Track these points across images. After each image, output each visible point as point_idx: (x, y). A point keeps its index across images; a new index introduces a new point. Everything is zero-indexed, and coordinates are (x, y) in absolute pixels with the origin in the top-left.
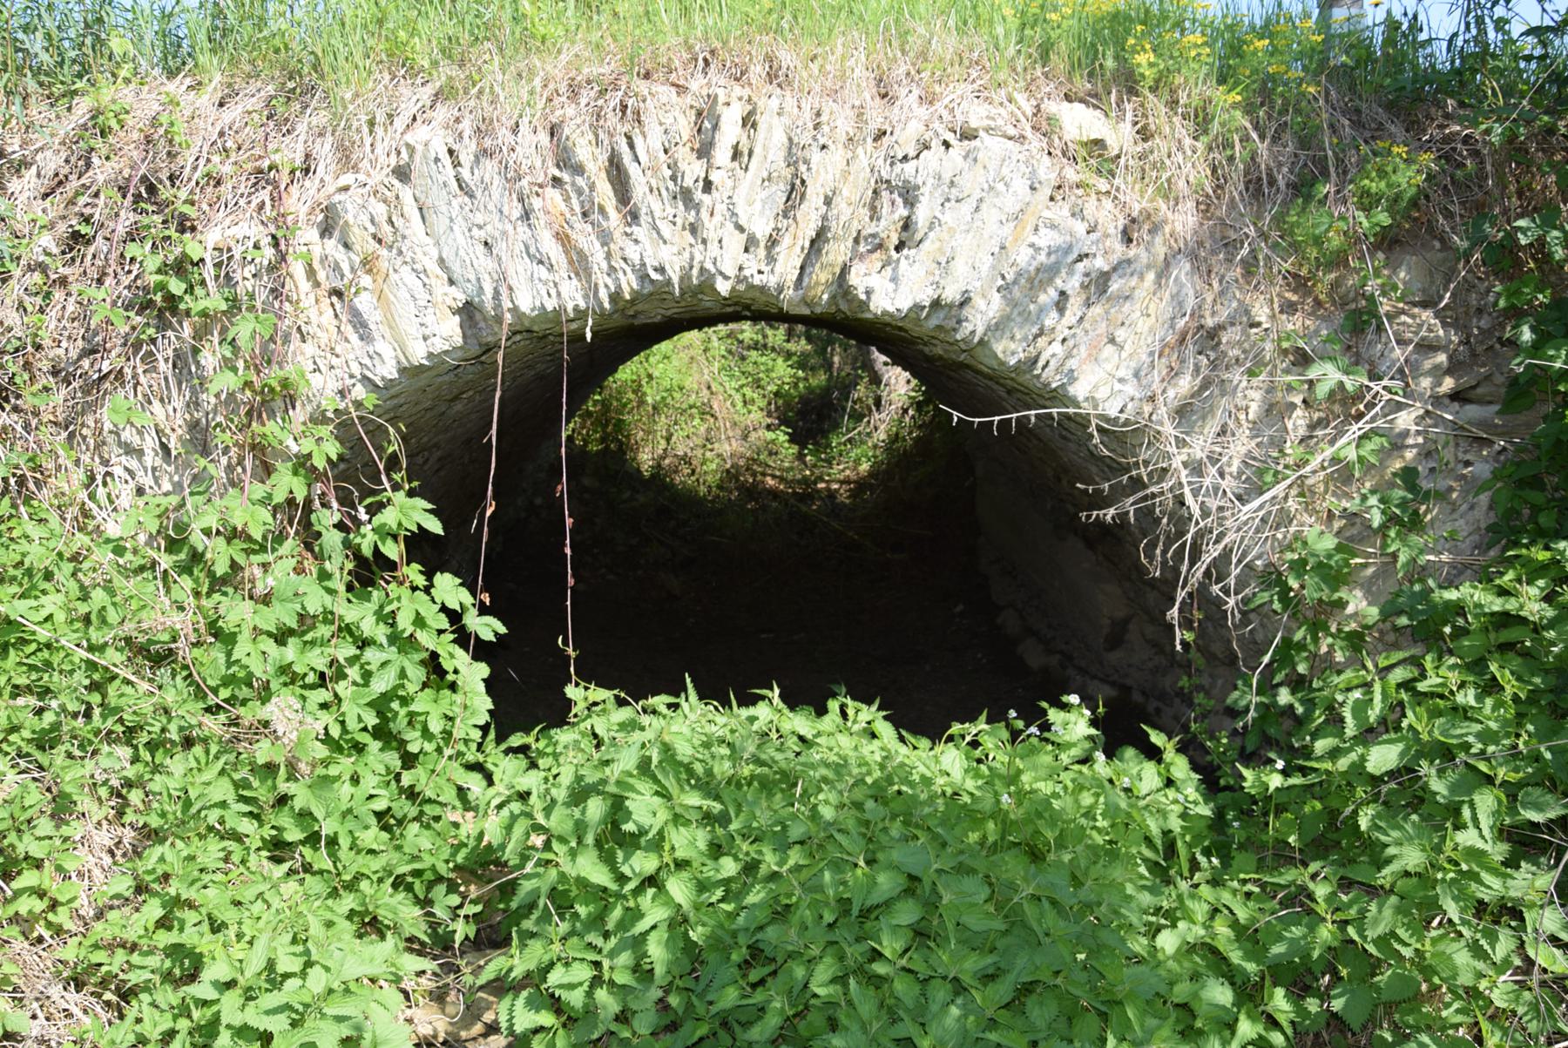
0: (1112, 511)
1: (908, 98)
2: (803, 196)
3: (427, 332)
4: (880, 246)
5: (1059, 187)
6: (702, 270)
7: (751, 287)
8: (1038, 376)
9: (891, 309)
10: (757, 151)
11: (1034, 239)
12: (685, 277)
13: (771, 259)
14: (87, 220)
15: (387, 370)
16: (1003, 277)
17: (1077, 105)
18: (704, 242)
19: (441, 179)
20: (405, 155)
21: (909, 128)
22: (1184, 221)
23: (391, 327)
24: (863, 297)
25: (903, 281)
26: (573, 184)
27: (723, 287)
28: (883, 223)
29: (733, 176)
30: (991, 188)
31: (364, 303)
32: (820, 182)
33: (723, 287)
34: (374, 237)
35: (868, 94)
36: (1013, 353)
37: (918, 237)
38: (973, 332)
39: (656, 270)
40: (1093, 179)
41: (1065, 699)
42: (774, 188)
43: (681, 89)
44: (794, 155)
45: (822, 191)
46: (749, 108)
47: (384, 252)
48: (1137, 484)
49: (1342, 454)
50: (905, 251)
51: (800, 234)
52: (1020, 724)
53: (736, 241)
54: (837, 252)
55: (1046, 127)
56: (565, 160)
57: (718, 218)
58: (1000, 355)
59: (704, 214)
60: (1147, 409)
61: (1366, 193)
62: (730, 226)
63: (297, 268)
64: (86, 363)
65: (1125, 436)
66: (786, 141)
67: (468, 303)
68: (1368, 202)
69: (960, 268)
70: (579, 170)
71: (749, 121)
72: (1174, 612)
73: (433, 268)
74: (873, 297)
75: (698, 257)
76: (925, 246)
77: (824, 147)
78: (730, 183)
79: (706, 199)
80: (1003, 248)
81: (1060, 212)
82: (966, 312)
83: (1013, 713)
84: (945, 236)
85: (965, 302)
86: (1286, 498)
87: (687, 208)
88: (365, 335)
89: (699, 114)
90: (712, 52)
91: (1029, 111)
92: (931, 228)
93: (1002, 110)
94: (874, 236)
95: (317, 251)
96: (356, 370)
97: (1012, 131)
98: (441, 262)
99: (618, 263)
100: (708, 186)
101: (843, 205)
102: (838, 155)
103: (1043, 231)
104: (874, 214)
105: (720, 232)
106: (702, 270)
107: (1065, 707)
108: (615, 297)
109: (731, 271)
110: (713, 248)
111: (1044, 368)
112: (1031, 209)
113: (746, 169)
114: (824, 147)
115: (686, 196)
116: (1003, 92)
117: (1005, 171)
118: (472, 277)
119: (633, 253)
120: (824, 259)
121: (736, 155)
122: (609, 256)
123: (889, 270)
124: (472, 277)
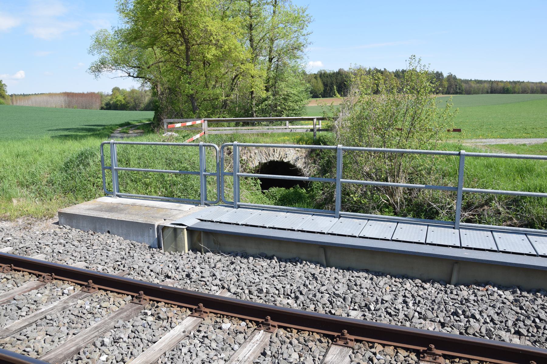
22: (304, 155)
54: (282, 158)
65: (300, 169)
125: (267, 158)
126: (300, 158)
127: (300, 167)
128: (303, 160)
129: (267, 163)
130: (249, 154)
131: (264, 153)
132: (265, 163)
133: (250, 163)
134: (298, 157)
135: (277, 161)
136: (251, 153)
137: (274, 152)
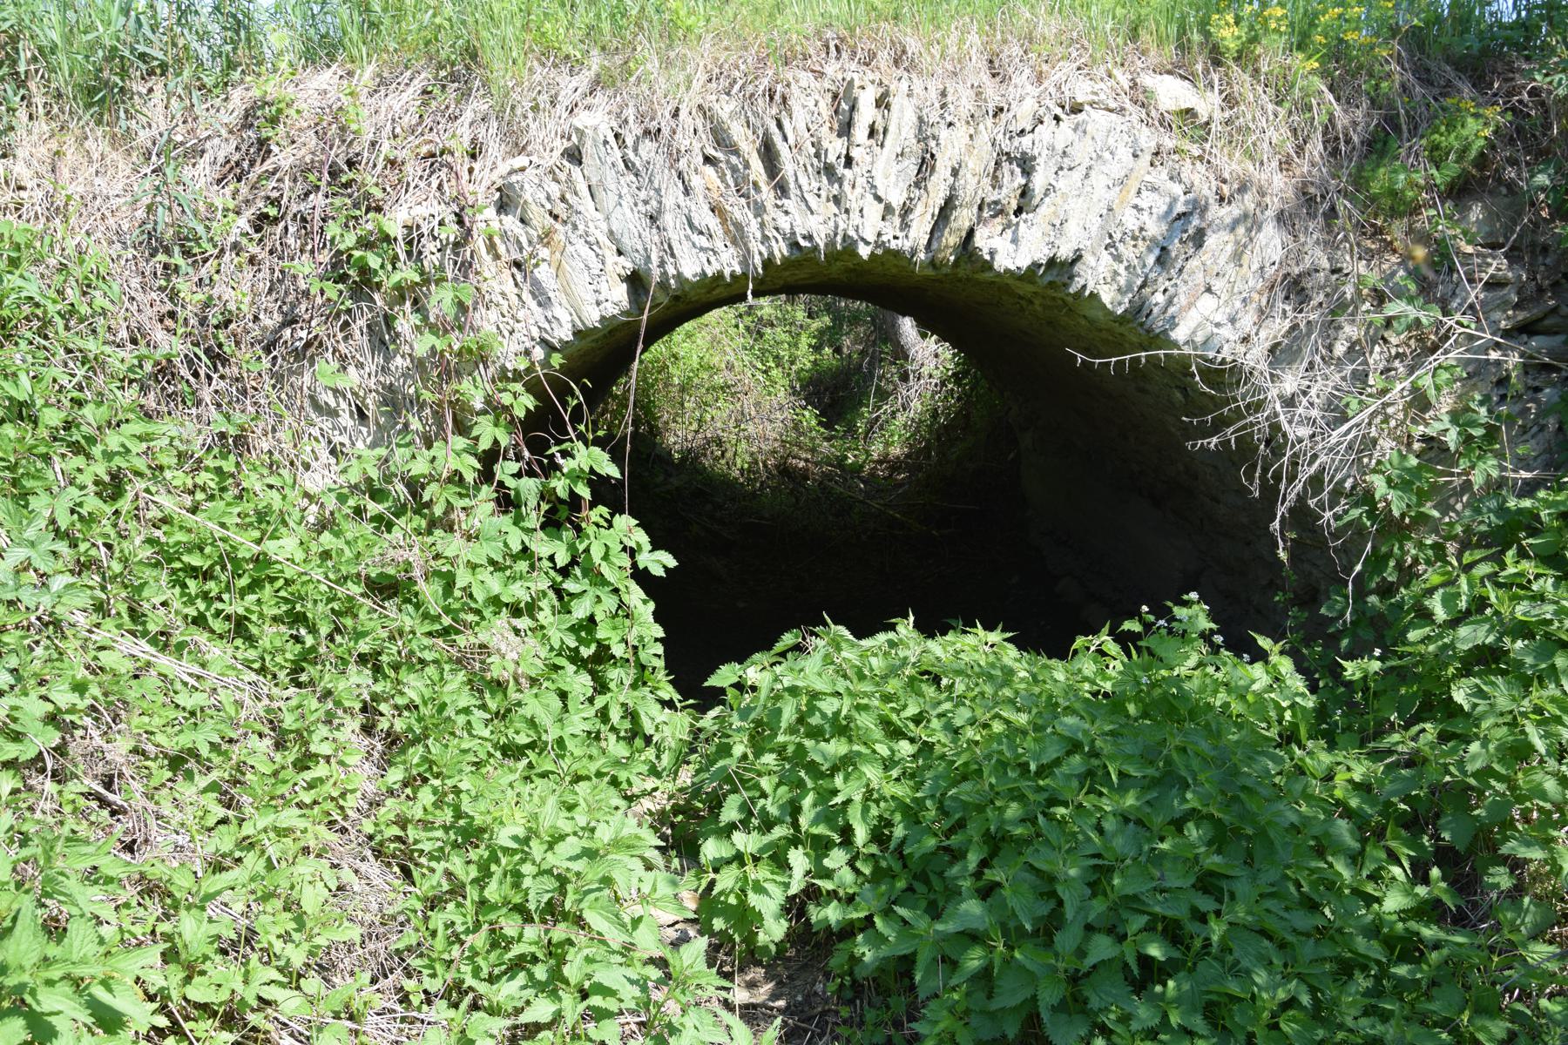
0: (1215, 440)
1: (1022, 79)
2: (933, 168)
3: (601, 298)
4: (1001, 212)
5: (1157, 154)
6: (846, 237)
7: (888, 251)
8: (1142, 324)
9: (1013, 268)
10: (892, 129)
11: (1137, 201)
12: (831, 243)
13: (905, 226)
14: (275, 202)
15: (564, 333)
16: (1111, 236)
17: (1166, 76)
18: (847, 211)
19: (609, 160)
20: (574, 139)
21: (1025, 102)
23: (567, 294)
24: (987, 257)
25: (1023, 243)
26: (728, 162)
27: (864, 251)
28: (1004, 190)
29: (870, 151)
30: (1099, 157)
31: (544, 273)
32: (948, 154)
33: (864, 251)
34: (551, 213)
35: (985, 77)
36: (1120, 304)
37: (1035, 201)
38: (1084, 287)
39: (804, 237)
40: (1186, 145)
41: (1185, 597)
42: (906, 162)
43: (820, 75)
44: (923, 129)
45: (949, 164)
46: (881, 90)
47: (558, 226)
49: (1420, 383)
50: (1024, 216)
51: (931, 202)
52: (1151, 618)
54: (963, 218)
55: (1142, 98)
56: (721, 138)
57: (859, 190)
58: (1109, 306)
59: (847, 187)
60: (1241, 349)
61: (1435, 147)
62: (870, 197)
63: (479, 244)
64: (287, 332)
65: (1224, 376)
66: (915, 119)
67: (634, 272)
68: (1437, 156)
69: (1072, 228)
71: (882, 103)
72: (1276, 524)
73: (604, 239)
74: (997, 257)
75: (842, 226)
76: (1042, 210)
77: (950, 124)
78: (868, 159)
79: (847, 172)
80: (1110, 210)
81: (1160, 176)
82: (1077, 268)
83: (1145, 608)
84: (1059, 201)
85: (1078, 258)
86: (1370, 424)
87: (831, 182)
88: (544, 302)
89: (835, 96)
90: (842, 40)
91: (1126, 85)
92: (1046, 195)
93: (1102, 85)
94: (996, 203)
95: (495, 225)
96: (536, 333)
97: (1113, 105)
98: (611, 232)
99: (771, 233)
100: (849, 162)
101: (969, 176)
102: (962, 131)
103: (1145, 193)
104: (996, 183)
105: (861, 203)
106: (846, 237)
107: (1187, 604)
108: (768, 263)
109: (871, 238)
110: (855, 218)
111: (1148, 316)
112: (1133, 176)
113: (882, 146)
114: (950, 124)
115: (829, 170)
116: (1102, 69)
117: (1111, 141)
118: (640, 248)
119: (783, 221)
120: (953, 225)
121: (872, 133)
122: (762, 225)
123: (1009, 232)
124: (640, 248)
125: (739, 210)
126: (1218, 213)
128: (1271, 243)
131: (692, 140)
133: (496, 279)
135: (890, 257)
137: (846, 129)
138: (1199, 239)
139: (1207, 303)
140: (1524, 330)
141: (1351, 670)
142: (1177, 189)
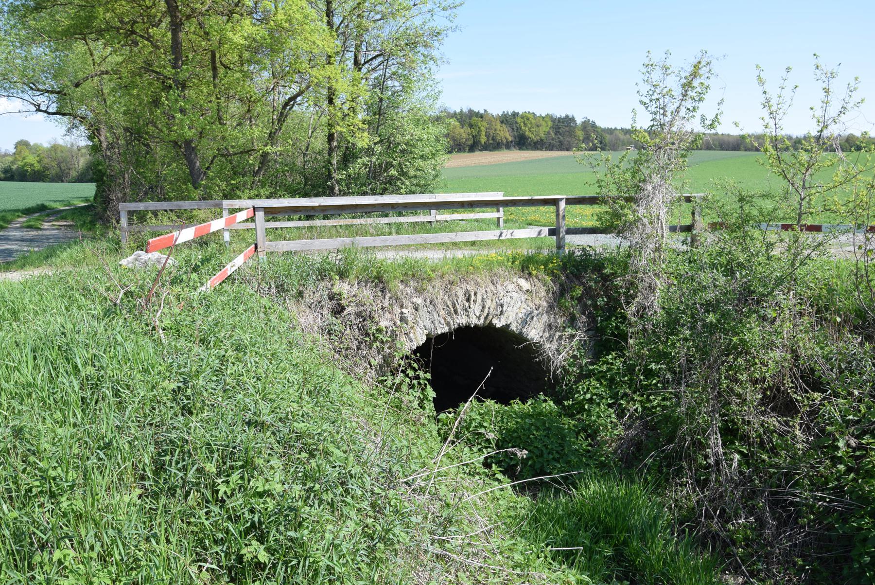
31: (411, 335)
33: (472, 326)
44: (483, 299)
48: (541, 354)
53: (474, 317)
55: (520, 288)
69: (510, 318)
70: (448, 306)
71: (475, 294)
88: (411, 341)
100: (470, 308)
115: (466, 310)
119: (458, 321)
125: (449, 319)
127: (536, 338)
128: (545, 318)
129: (450, 333)
130: (397, 310)
132: (443, 335)
134: (531, 313)
135: (476, 326)
136: (402, 307)
137: (468, 300)
138: (532, 318)
139: (534, 330)
140: (588, 330)
141: (566, 403)
142: (529, 309)
